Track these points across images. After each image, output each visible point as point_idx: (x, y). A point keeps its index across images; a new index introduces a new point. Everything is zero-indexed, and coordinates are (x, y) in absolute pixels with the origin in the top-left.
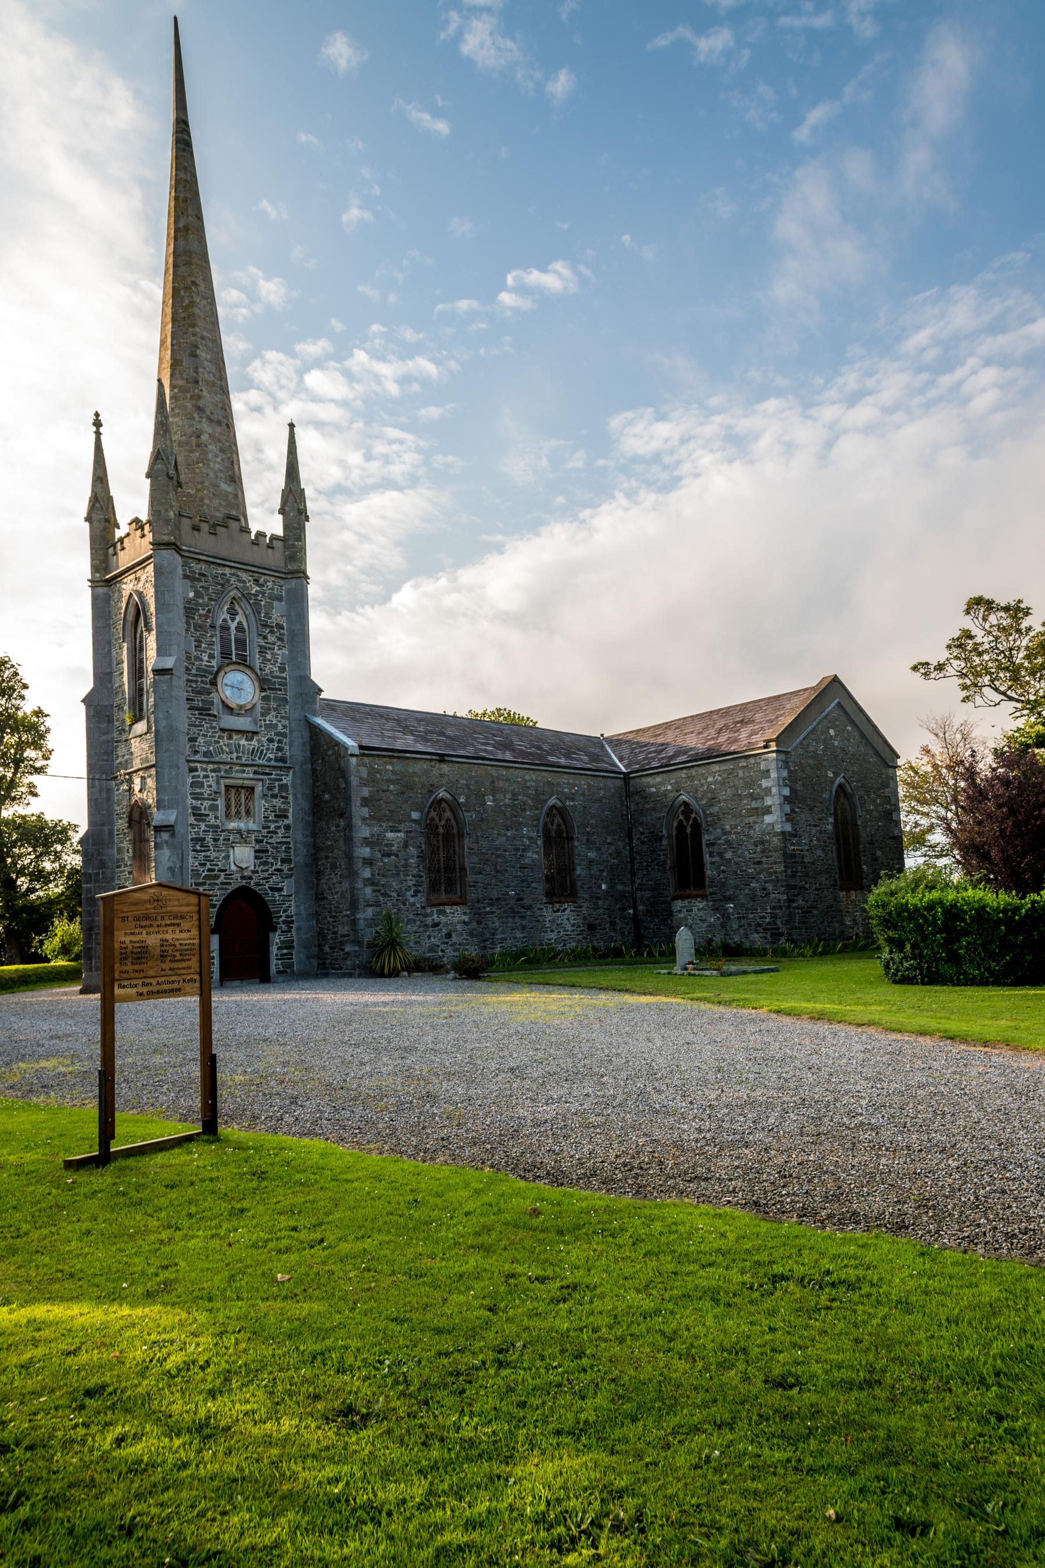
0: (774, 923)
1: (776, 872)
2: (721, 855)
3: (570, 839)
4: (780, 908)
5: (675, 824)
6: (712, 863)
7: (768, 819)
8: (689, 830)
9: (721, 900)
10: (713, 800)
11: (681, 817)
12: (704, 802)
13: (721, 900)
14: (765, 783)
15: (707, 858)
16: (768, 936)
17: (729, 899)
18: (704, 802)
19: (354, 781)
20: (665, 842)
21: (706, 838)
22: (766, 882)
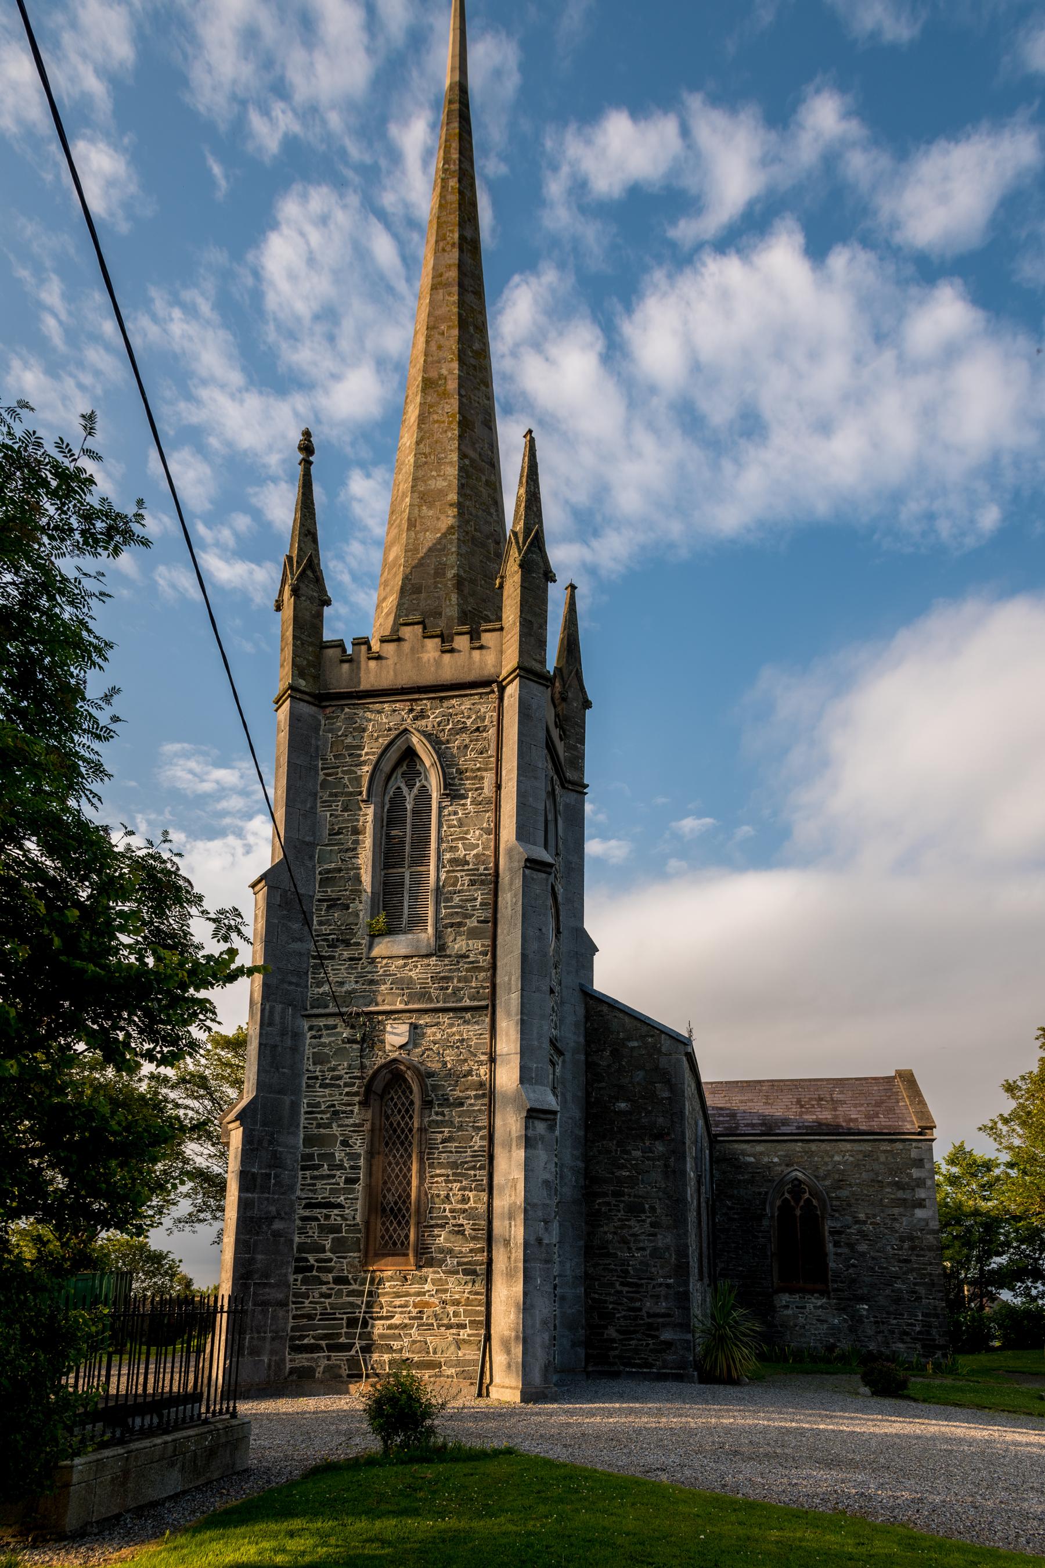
0: (928, 1333)
1: (931, 1274)
2: (851, 1246)
4: (937, 1316)
5: (778, 1203)
6: (836, 1254)
7: (919, 1213)
8: (798, 1212)
9: (849, 1299)
11: (787, 1195)
12: (827, 1183)
13: (849, 1299)
15: (830, 1247)
16: (919, 1346)
17: (862, 1299)
18: (827, 1183)
20: (765, 1222)
21: (829, 1224)
22: (915, 1284)
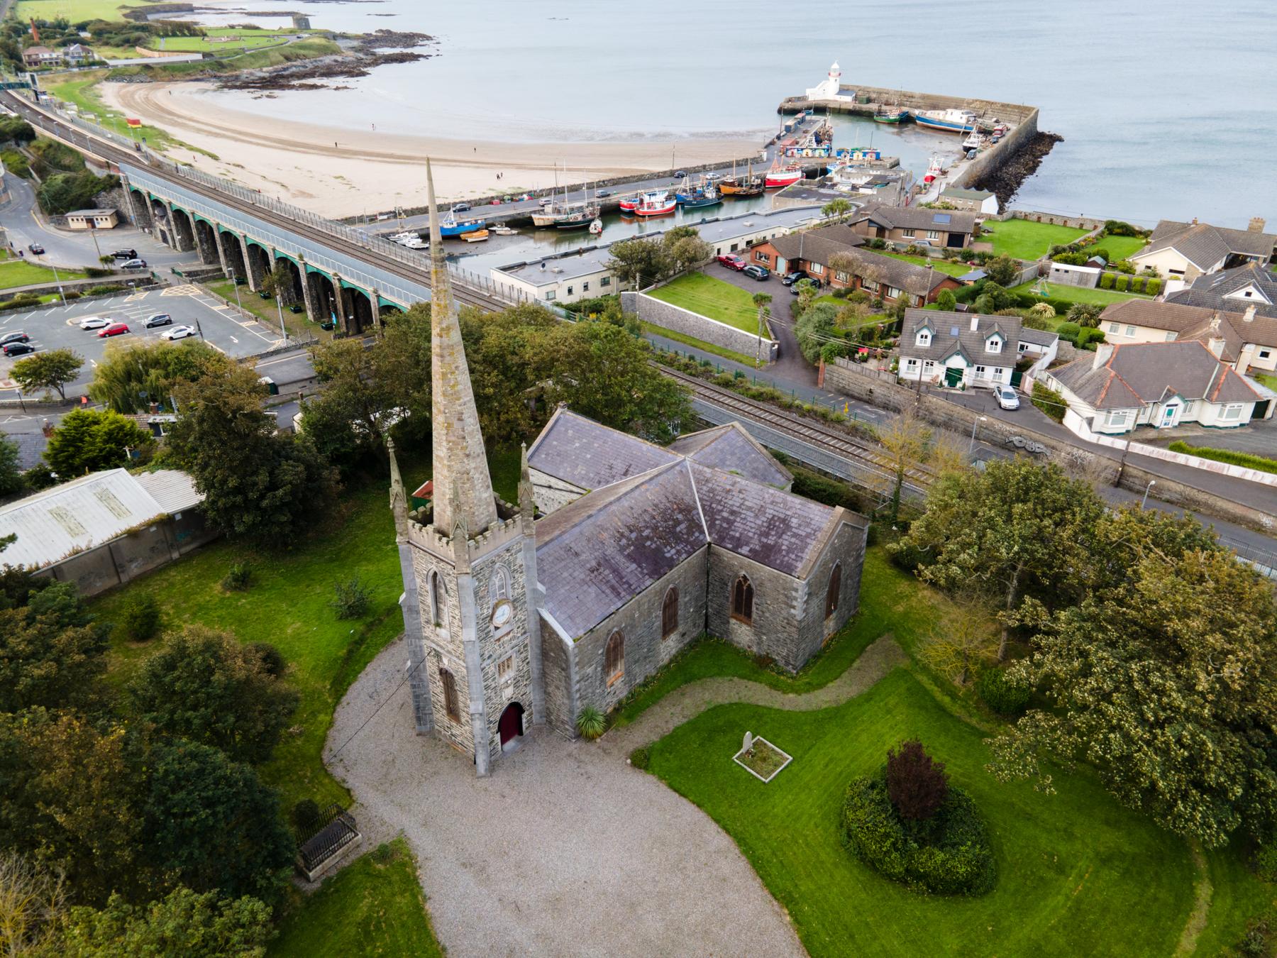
3: (676, 600)
10: (761, 584)
14: (794, 594)
15: (754, 609)
19: (571, 659)
21: (754, 600)
